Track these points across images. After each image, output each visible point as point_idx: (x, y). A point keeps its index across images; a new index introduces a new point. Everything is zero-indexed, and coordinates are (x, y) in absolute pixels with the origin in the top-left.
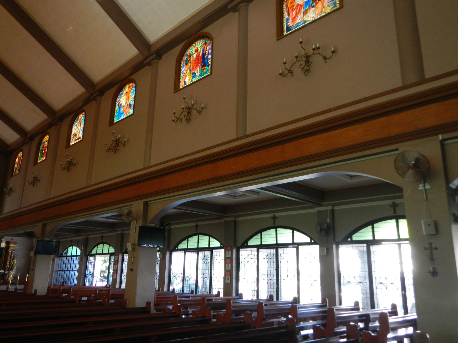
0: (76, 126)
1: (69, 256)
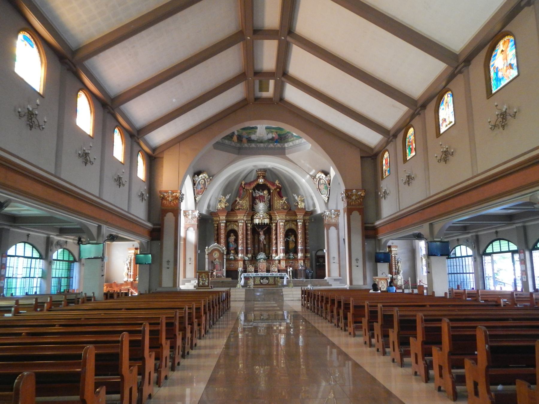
0: (443, 109)
1: (459, 257)
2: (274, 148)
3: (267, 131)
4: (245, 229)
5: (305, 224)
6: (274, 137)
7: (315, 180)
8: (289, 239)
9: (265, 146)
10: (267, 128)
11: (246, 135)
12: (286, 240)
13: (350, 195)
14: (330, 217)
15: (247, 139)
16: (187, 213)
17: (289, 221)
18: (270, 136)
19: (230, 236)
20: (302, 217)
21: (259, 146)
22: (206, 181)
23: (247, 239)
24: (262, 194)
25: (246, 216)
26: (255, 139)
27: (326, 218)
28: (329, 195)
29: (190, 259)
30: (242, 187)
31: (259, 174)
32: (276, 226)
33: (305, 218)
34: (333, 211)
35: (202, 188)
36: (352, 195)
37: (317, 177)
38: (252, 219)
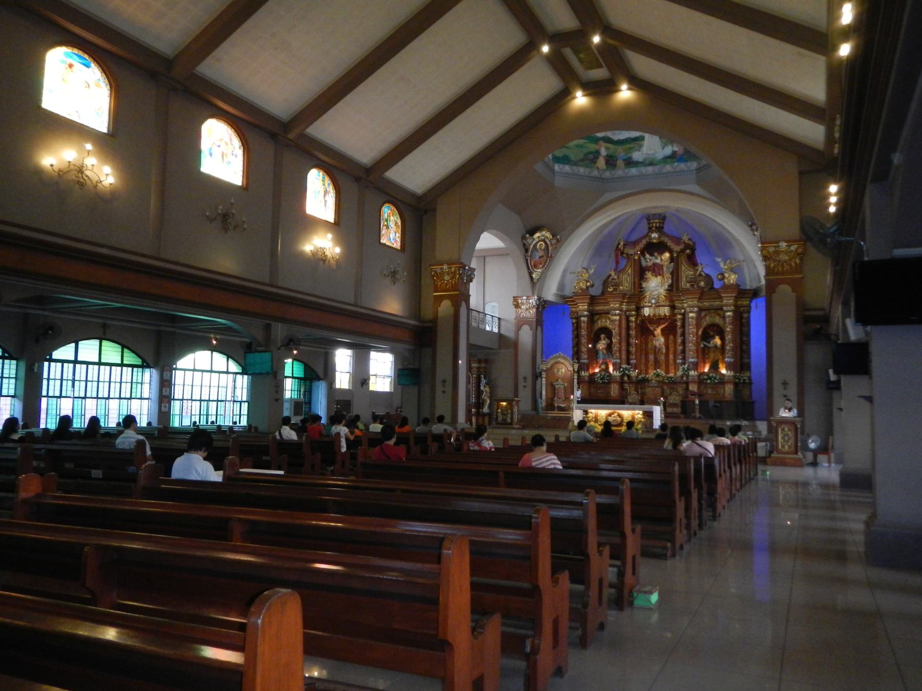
2: (673, 173)
3: (662, 142)
8: (709, 343)
11: (623, 153)
15: (624, 160)
18: (668, 150)
19: (600, 339)
20: (732, 301)
22: (549, 243)
23: (628, 344)
24: (658, 261)
26: (641, 160)
29: (525, 378)
30: (620, 250)
32: (684, 320)
35: (543, 256)
36: (777, 252)
38: (639, 309)
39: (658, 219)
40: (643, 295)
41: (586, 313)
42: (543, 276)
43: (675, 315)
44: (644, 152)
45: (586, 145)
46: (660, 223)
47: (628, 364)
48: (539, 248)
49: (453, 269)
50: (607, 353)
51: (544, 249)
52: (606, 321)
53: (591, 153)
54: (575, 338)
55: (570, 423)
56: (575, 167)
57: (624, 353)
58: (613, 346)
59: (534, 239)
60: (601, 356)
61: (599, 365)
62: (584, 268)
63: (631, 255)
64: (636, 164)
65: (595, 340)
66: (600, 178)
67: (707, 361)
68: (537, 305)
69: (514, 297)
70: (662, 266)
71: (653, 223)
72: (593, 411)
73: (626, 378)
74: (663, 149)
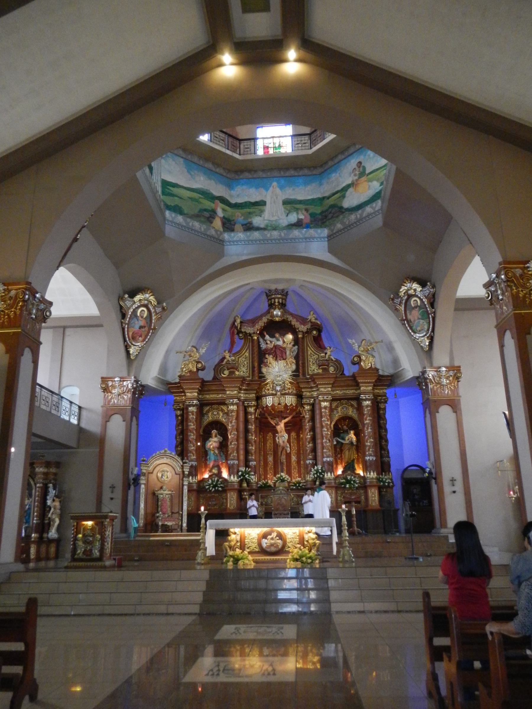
3: (285, 208)
4: (242, 418)
5: (378, 406)
6: (302, 219)
7: (397, 301)
8: (343, 439)
9: (283, 235)
10: (286, 202)
11: (243, 218)
12: (335, 443)
13: (521, 275)
14: (439, 383)
15: (243, 225)
16: (110, 383)
17: (340, 400)
18: (293, 218)
20: (371, 388)
21: (269, 235)
23: (247, 442)
24: (280, 343)
25: (245, 390)
26: (262, 226)
27: (427, 385)
28: (433, 331)
29: (113, 487)
30: (236, 327)
31: (271, 299)
32: (313, 411)
33: (377, 391)
34: (444, 369)
35: (145, 327)
37: (402, 294)
38: (258, 398)
39: (281, 294)
40: (265, 380)
41: (195, 402)
42: (143, 351)
43: (302, 405)
44: (266, 218)
45: (200, 200)
46: (282, 299)
47: (247, 466)
48: (140, 315)
49: (13, 293)
50: (219, 453)
51: (146, 317)
52: (218, 414)
53: (205, 210)
54: (179, 435)
55: (200, 553)
56: (189, 220)
57: (242, 452)
58: (229, 444)
59: (134, 302)
60: (212, 457)
61: (208, 469)
62: (193, 346)
63: (250, 335)
64: (258, 229)
65: (205, 436)
66: (217, 239)
67: (339, 461)
68: (133, 388)
69: (102, 378)
70: (285, 349)
71: (274, 298)
72: (237, 530)
73: (245, 485)
74: (287, 216)
